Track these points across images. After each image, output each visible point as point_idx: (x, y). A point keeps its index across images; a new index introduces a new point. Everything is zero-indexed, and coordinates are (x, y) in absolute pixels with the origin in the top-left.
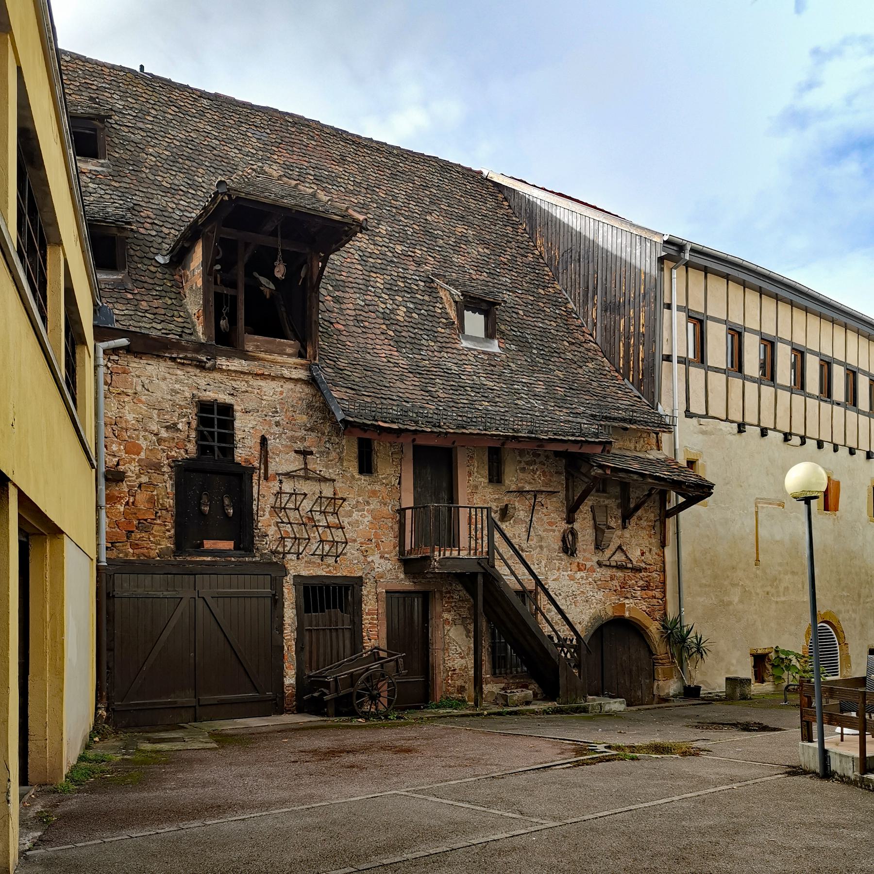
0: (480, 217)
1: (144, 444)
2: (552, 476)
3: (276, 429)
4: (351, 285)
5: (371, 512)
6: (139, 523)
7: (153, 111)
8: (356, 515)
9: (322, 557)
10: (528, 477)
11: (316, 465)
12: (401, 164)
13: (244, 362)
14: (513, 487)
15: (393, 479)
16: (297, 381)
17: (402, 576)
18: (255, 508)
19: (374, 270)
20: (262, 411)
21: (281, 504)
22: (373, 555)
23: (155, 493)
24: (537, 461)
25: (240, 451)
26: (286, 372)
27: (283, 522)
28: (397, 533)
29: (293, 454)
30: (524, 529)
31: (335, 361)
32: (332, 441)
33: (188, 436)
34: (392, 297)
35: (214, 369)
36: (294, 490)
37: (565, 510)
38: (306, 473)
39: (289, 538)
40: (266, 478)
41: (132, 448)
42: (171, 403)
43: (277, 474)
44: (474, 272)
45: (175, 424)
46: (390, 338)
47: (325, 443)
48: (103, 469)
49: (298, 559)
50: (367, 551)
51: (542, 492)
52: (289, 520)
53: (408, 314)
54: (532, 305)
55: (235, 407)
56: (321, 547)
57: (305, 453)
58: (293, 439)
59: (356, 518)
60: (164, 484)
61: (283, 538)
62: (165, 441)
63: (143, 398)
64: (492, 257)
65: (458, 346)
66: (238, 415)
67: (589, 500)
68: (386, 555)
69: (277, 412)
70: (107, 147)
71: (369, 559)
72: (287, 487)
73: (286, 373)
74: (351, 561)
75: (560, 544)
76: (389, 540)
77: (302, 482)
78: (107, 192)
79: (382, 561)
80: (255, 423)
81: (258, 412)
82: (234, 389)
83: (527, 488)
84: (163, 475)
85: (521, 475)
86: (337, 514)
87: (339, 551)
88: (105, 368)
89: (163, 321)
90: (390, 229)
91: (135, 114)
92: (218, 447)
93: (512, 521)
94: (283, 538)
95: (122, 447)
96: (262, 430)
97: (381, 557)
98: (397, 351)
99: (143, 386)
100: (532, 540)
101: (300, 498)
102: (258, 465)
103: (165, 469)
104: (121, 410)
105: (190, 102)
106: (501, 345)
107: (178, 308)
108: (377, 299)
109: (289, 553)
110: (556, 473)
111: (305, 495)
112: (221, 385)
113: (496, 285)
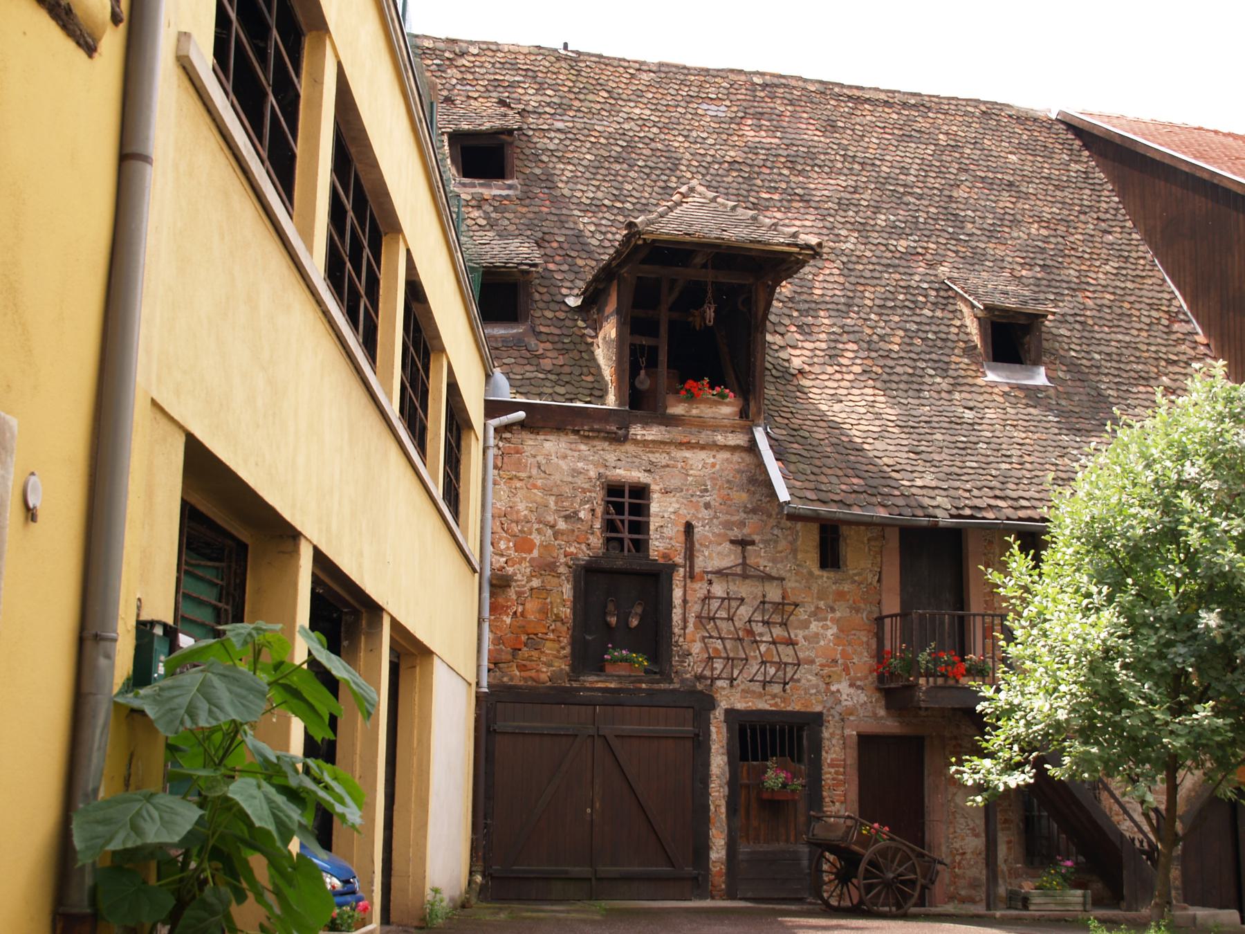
1: (536, 539)
3: (705, 513)
5: (836, 621)
7: (577, 103)
8: (815, 626)
9: (765, 684)
11: (760, 558)
13: (663, 428)
15: (870, 576)
16: (734, 449)
17: (882, 712)
19: (862, 281)
20: (687, 490)
22: (839, 682)
25: (657, 543)
26: (719, 437)
27: (711, 637)
28: (874, 653)
29: (727, 545)
32: (782, 525)
34: (884, 318)
36: (728, 593)
38: (744, 570)
39: (720, 658)
42: (571, 486)
45: (576, 513)
46: (876, 377)
47: (772, 528)
48: (488, 573)
49: (732, 686)
52: (719, 634)
53: (907, 340)
54: (1110, 307)
55: (653, 487)
57: (743, 543)
59: (815, 630)
61: (710, 658)
62: (562, 534)
63: (539, 483)
64: (1052, 239)
65: (980, 381)
66: (655, 496)
68: (859, 683)
69: (706, 490)
70: (517, 162)
71: (833, 688)
72: (718, 590)
73: (720, 439)
74: (806, 690)
76: (863, 660)
78: (512, 221)
79: (852, 691)
80: (677, 506)
81: (682, 491)
82: (651, 463)
84: (559, 577)
86: (785, 625)
87: (789, 675)
88: (496, 449)
89: (567, 382)
90: (892, 218)
91: (553, 111)
92: (631, 540)
94: (710, 658)
95: (511, 544)
96: (687, 514)
97: (851, 685)
99: (539, 467)
101: (734, 604)
105: (625, 81)
106: (1050, 375)
107: (588, 364)
108: (860, 322)
109: (718, 678)
111: (742, 600)
112: (635, 460)
113: (1054, 283)
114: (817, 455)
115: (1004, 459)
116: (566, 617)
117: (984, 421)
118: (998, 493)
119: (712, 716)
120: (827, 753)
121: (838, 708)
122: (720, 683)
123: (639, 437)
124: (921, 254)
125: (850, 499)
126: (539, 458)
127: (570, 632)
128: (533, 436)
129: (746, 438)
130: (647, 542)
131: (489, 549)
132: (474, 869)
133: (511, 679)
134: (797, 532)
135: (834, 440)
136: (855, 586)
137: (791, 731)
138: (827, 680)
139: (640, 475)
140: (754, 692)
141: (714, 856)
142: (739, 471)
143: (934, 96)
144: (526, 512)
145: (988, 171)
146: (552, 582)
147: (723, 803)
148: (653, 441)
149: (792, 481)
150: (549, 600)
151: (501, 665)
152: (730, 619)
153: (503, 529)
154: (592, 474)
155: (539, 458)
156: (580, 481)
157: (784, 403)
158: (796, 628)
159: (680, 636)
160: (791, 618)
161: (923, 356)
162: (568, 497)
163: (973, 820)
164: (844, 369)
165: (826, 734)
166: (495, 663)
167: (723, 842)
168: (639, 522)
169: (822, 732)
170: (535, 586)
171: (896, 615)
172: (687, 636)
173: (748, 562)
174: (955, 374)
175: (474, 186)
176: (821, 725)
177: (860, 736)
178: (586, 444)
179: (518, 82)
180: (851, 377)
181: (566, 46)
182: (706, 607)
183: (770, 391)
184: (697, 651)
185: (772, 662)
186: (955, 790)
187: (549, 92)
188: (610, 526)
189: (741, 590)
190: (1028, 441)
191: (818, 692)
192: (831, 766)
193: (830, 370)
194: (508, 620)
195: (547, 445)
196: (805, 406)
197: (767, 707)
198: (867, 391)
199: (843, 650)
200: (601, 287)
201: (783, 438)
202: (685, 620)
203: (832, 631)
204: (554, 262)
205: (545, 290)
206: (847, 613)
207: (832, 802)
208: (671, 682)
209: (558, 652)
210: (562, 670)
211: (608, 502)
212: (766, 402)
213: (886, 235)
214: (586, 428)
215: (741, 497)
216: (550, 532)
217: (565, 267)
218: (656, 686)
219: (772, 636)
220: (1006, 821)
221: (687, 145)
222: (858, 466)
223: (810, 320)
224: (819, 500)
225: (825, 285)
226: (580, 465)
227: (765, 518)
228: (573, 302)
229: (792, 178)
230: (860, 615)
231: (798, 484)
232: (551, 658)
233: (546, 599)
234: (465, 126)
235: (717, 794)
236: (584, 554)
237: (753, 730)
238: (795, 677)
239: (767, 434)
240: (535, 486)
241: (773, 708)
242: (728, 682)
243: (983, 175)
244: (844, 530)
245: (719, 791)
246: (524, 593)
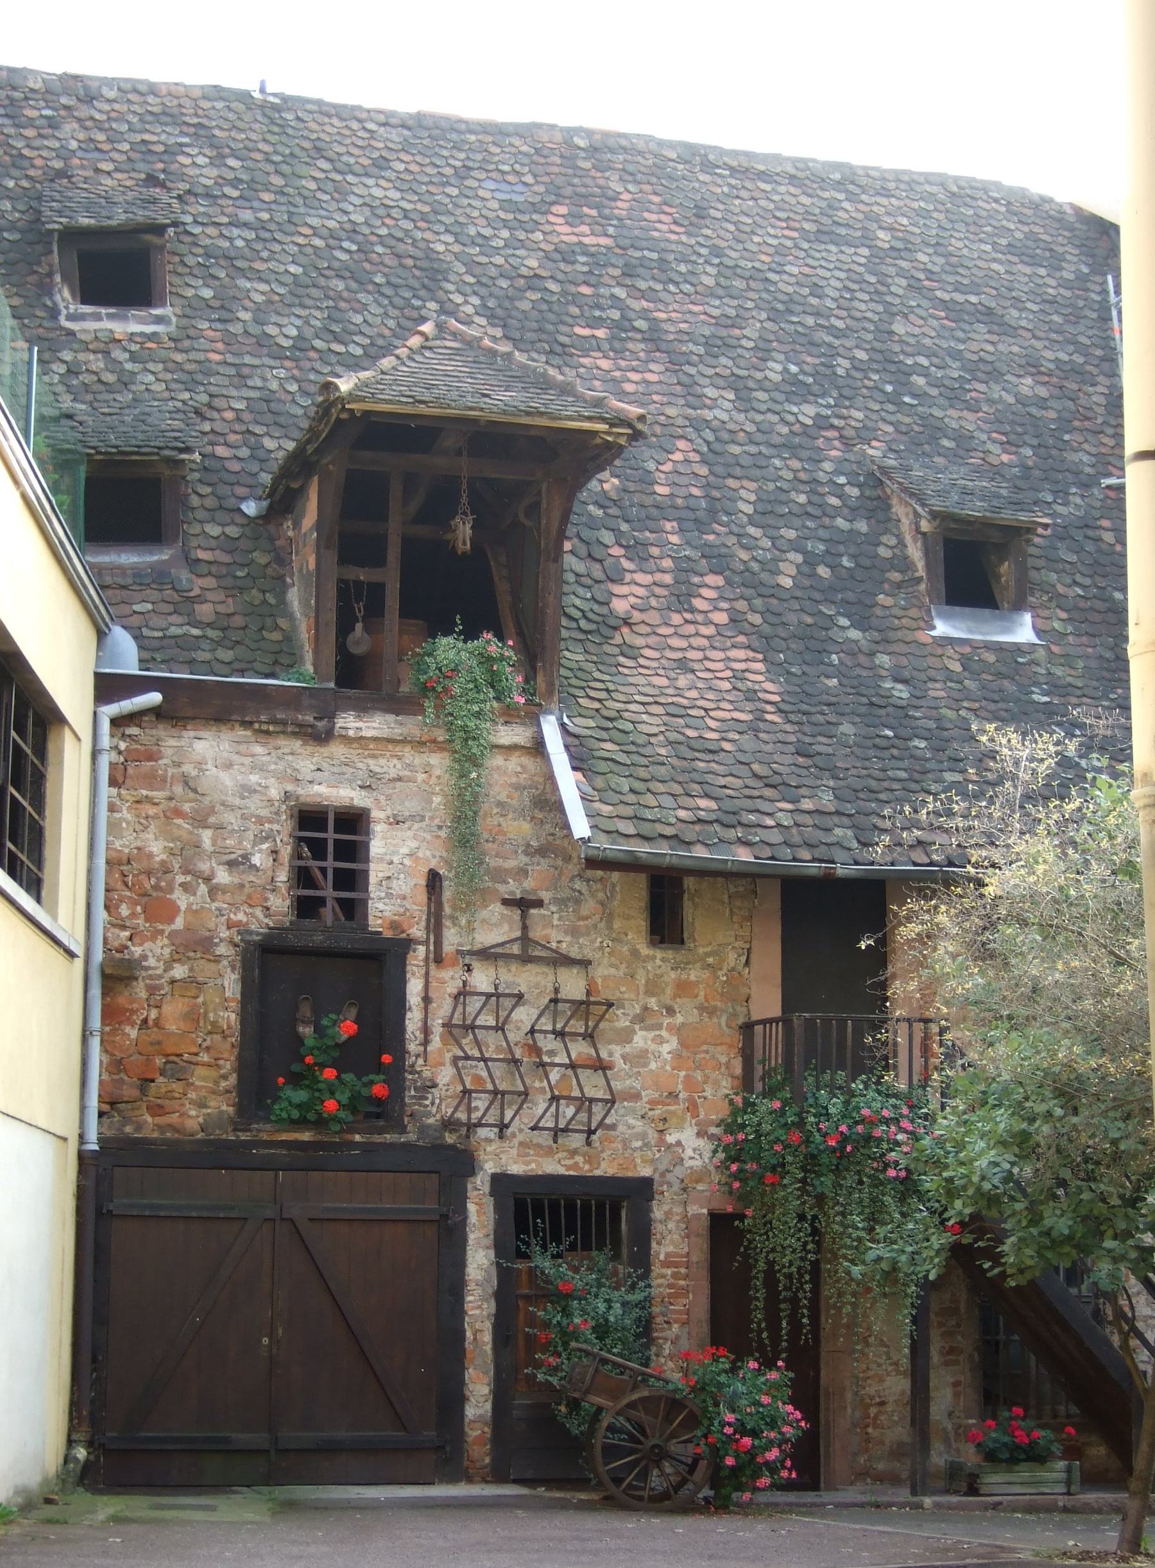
0: (1035, 308)
1: (182, 900)
5: (678, 1030)
7: (278, 181)
8: (641, 1039)
12: (846, 205)
13: (391, 718)
15: (732, 957)
19: (738, 471)
20: (432, 818)
21: (464, 1019)
22: (680, 1128)
25: (381, 906)
27: (467, 1058)
31: (600, 701)
38: (524, 948)
40: (439, 960)
43: (459, 952)
44: (995, 449)
45: (246, 857)
47: (572, 879)
48: (98, 956)
49: (501, 1136)
55: (375, 814)
56: (553, 1109)
57: (524, 905)
59: (641, 1044)
62: (224, 892)
63: (187, 807)
65: (923, 636)
66: (378, 828)
71: (671, 1139)
72: (482, 979)
74: (625, 1143)
78: (160, 376)
80: (414, 844)
81: (422, 819)
82: (372, 774)
86: (591, 1036)
88: (114, 754)
90: (794, 369)
94: (466, 1092)
95: (139, 909)
98: (765, 660)
99: (186, 783)
101: (507, 1003)
103: (222, 950)
104: (142, 835)
105: (360, 143)
111: (520, 996)
112: (345, 769)
114: (644, 761)
116: (229, 1027)
119: (469, 1186)
120: (659, 1243)
122: (483, 1132)
123: (351, 733)
125: (690, 834)
127: (236, 1051)
128: (174, 732)
130: (364, 903)
132: (74, 1437)
134: (614, 886)
135: (673, 736)
136: (706, 974)
137: (601, 1207)
138: (661, 1127)
139: (353, 794)
140: (539, 1146)
141: (470, 1412)
142: (517, 787)
143: (872, 168)
144: (164, 857)
145: (956, 290)
146: (205, 969)
147: (488, 1326)
148: (375, 739)
149: (597, 805)
150: (200, 1000)
151: (122, 1106)
152: (500, 1028)
153: (126, 884)
154: (275, 793)
156: (255, 805)
157: (597, 675)
158: (610, 1042)
159: (418, 1056)
160: (602, 1025)
164: (700, 618)
165: (657, 1213)
167: (485, 1390)
168: (353, 871)
169: (650, 1210)
171: (771, 1021)
172: (430, 1058)
173: (531, 935)
175: (98, 317)
176: (652, 1199)
178: (264, 744)
179: (181, 145)
180: (710, 631)
181: (262, 90)
182: (460, 1008)
183: (573, 656)
184: (446, 1080)
188: (302, 877)
189: (519, 980)
191: (646, 1145)
192: (666, 1264)
193: (676, 619)
194: (133, 1033)
195: (199, 746)
196: (631, 680)
197: (562, 1171)
198: (733, 653)
199: (687, 1077)
200: (295, 485)
201: (588, 732)
202: (426, 1030)
203: (670, 1045)
204: (226, 444)
205: (209, 490)
206: (694, 1016)
207: (667, 1322)
208: (403, 1130)
209: (216, 1083)
211: (301, 839)
212: (563, 672)
214: (263, 718)
216: (203, 889)
217: (244, 452)
218: (377, 1139)
219: (569, 1056)
220: (951, 1351)
221: (457, 248)
222: (709, 778)
226: (254, 778)
227: (560, 863)
228: (250, 508)
230: (715, 1020)
231: (606, 809)
232: (203, 1093)
233: (196, 997)
234: (85, 221)
235: (477, 1312)
236: (258, 922)
238: (608, 1121)
239: (563, 726)
240: (179, 813)
241: (572, 1173)
242: (496, 1130)
244: (689, 882)
245: (479, 1307)
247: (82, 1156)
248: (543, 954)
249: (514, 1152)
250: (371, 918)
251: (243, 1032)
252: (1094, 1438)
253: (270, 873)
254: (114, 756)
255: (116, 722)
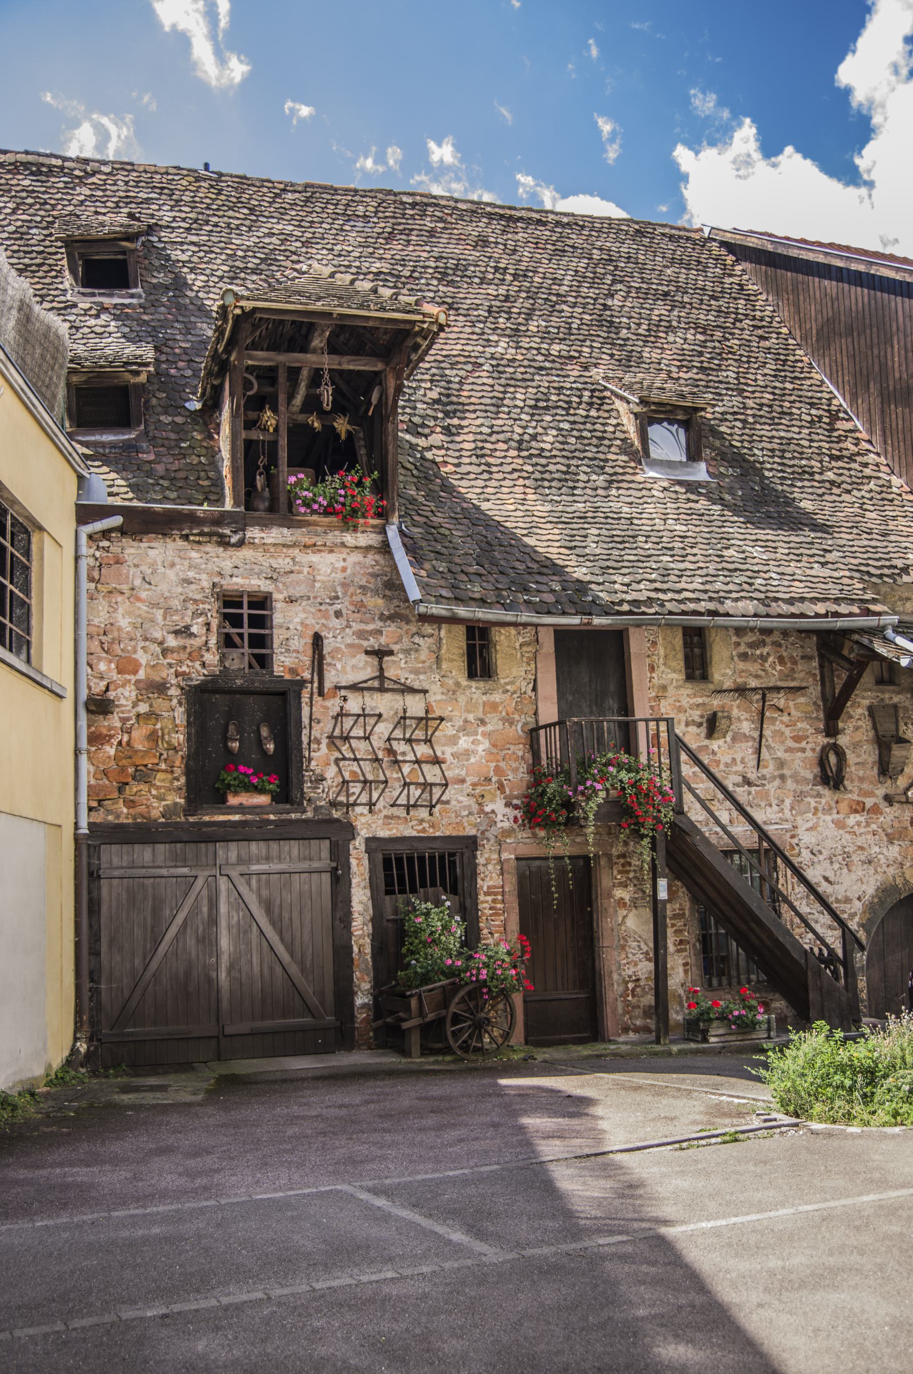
1: (142, 658)
2: (795, 663)
3: (336, 623)
4: (471, 408)
6: (136, 770)
8: (464, 742)
9: (408, 807)
10: (753, 667)
11: (397, 669)
13: (285, 530)
14: (728, 684)
15: (524, 684)
18: (305, 739)
19: (512, 382)
20: (315, 598)
22: (493, 801)
23: (158, 726)
24: (768, 640)
25: (283, 659)
27: (344, 759)
29: (363, 657)
30: (750, 751)
33: (206, 642)
34: (536, 418)
35: (241, 544)
36: (363, 709)
37: (822, 716)
38: (382, 683)
41: (127, 666)
45: (187, 627)
49: (371, 811)
50: (483, 796)
51: (778, 689)
53: (560, 439)
55: (276, 596)
56: (406, 791)
57: (380, 654)
58: (361, 635)
59: (465, 746)
60: (171, 714)
63: (144, 595)
65: (639, 478)
66: (278, 605)
67: (863, 698)
69: (337, 598)
72: (354, 704)
75: (817, 770)
77: (377, 696)
80: (303, 615)
83: (753, 683)
85: (741, 665)
86: (430, 741)
90: (544, 324)
93: (728, 739)
94: (344, 782)
95: (113, 666)
97: (507, 805)
99: (144, 579)
100: (767, 767)
102: (309, 676)
106: (711, 470)
110: (803, 658)
111: (380, 716)
113: (711, 384)
115: (665, 551)
116: (179, 744)
117: (644, 516)
118: (658, 585)
119: (351, 847)
120: (483, 880)
121: (494, 831)
122: (359, 810)
124: (575, 358)
126: (144, 568)
128: (135, 544)
129: (380, 538)
131: (84, 669)
132: (78, 1035)
133: (118, 817)
137: (442, 857)
139: (260, 583)
142: (375, 575)
146: (160, 704)
151: (105, 803)
152: (367, 738)
155: (143, 568)
158: (444, 745)
161: (577, 454)
162: (177, 611)
163: (646, 944)
165: (481, 860)
166: (99, 801)
169: (475, 857)
170: (142, 711)
173: (386, 674)
174: (611, 471)
175: (93, 295)
177: (517, 859)
178: (198, 551)
182: (339, 724)
184: (332, 775)
185: (417, 784)
186: (625, 913)
187: (187, 209)
190: (690, 534)
191: (470, 814)
192: (487, 894)
195: (152, 553)
200: (216, 382)
203: (485, 745)
207: (491, 933)
209: (172, 783)
210: (176, 804)
213: (538, 340)
214: (195, 532)
215: (376, 603)
220: (681, 942)
223: (455, 421)
224: (456, 598)
225: (475, 387)
226: (191, 574)
229: (441, 288)
236: (198, 674)
237: (399, 860)
238: (444, 798)
240: (139, 599)
243: (637, 285)
246: (128, 719)
247: (77, 839)
248: (396, 686)
249: (381, 822)
250: (275, 666)
251: (189, 748)
252: (777, 996)
253: (204, 638)
254: (91, 561)
255: (90, 537)
